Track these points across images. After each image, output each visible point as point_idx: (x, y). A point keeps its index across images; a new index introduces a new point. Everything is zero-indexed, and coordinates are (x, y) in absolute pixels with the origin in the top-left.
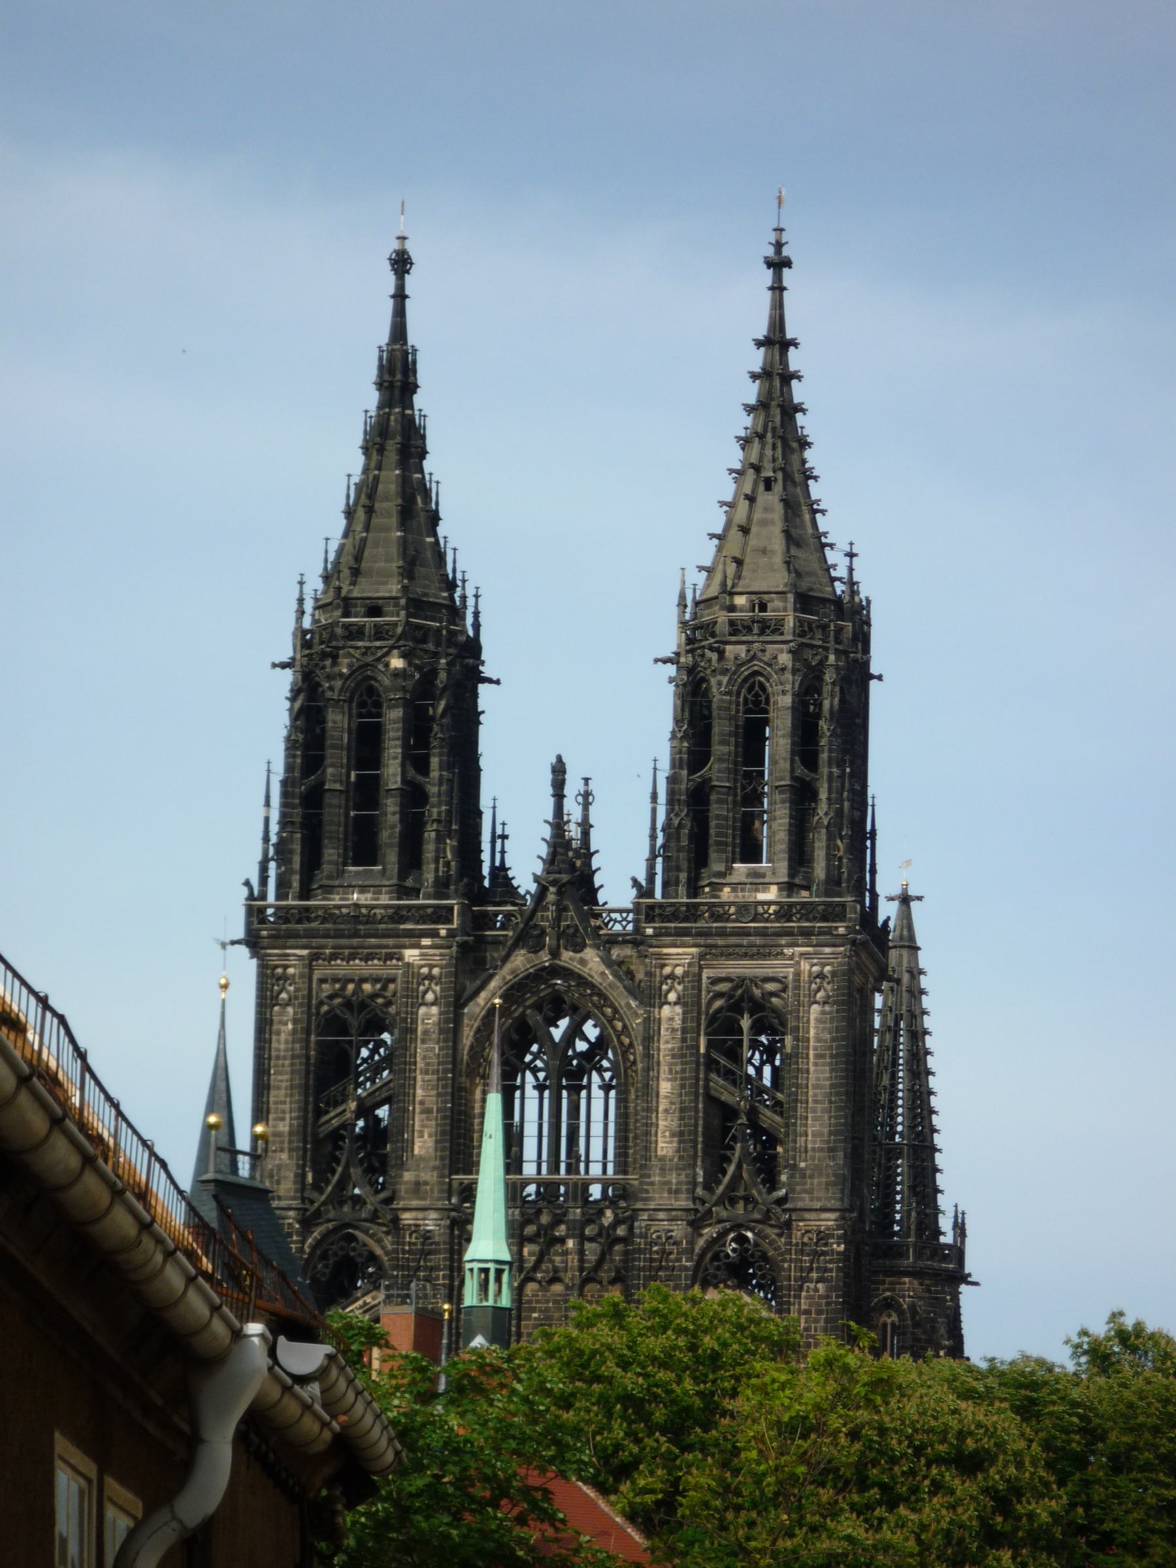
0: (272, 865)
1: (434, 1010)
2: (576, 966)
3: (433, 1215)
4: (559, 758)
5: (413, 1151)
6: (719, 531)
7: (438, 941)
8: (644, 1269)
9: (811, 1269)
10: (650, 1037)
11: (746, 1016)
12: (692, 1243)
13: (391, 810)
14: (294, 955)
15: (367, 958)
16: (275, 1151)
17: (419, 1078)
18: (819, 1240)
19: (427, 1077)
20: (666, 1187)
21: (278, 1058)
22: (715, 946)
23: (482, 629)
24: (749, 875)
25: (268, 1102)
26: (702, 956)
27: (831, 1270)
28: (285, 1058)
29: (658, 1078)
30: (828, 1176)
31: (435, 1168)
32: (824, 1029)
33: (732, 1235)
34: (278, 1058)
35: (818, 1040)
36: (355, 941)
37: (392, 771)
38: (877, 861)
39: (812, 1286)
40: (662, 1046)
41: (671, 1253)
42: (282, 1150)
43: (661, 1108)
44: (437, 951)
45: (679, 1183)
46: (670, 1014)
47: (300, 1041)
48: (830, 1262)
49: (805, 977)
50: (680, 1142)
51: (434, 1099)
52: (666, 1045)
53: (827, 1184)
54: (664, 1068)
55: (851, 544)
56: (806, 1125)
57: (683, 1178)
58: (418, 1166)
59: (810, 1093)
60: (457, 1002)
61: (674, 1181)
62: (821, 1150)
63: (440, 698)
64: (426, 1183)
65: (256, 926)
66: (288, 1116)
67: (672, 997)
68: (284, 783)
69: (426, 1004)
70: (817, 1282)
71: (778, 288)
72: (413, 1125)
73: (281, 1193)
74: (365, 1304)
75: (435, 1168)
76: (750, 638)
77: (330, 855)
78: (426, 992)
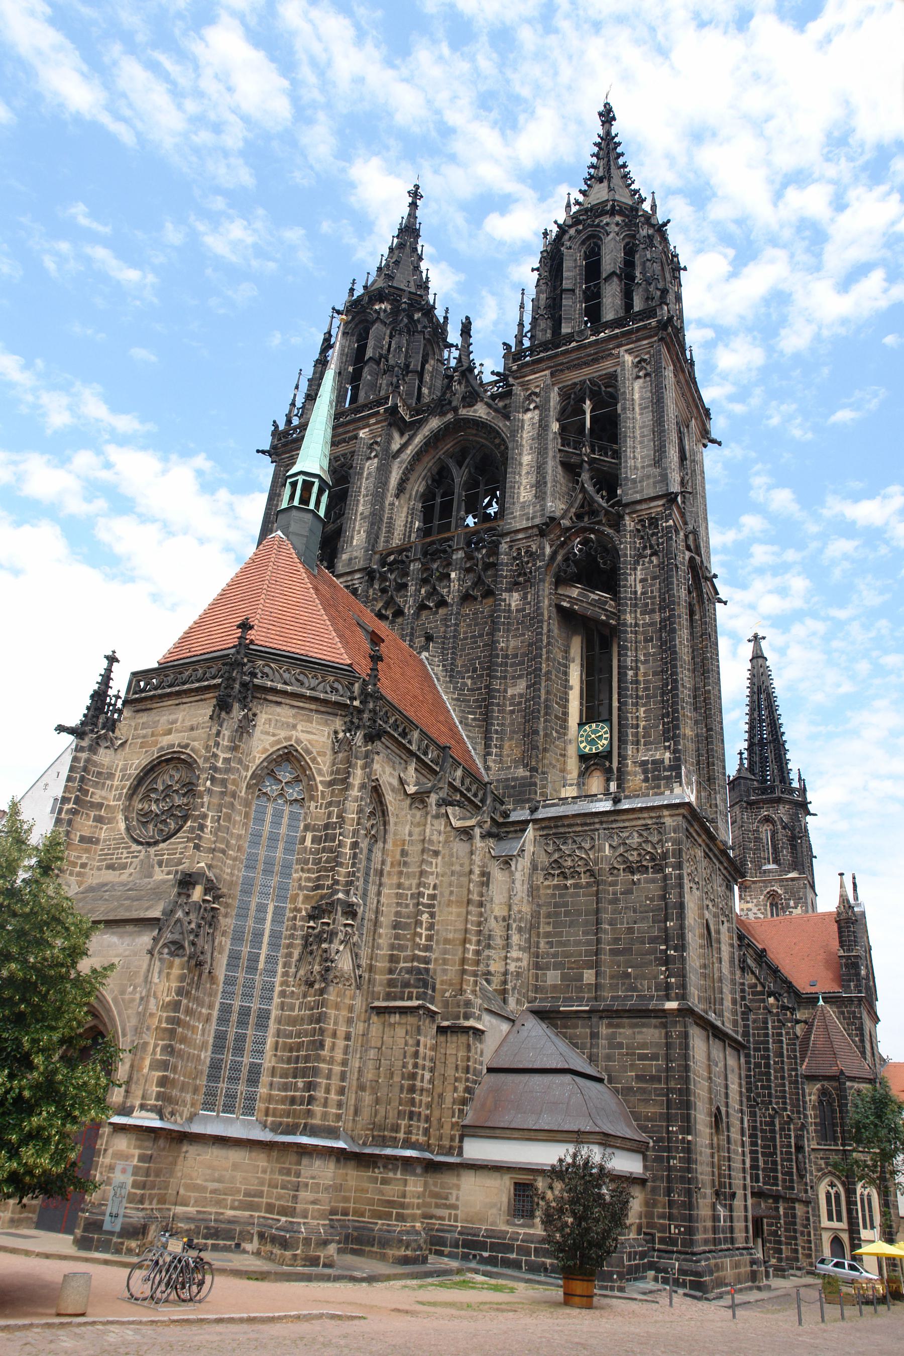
4: (467, 318)
8: (506, 577)
11: (588, 402)
22: (562, 364)
29: (520, 454)
35: (642, 398)
39: (647, 560)
40: (525, 436)
43: (524, 472)
45: (534, 512)
48: (662, 537)
52: (527, 435)
53: (654, 483)
54: (526, 449)
59: (638, 432)
62: (650, 466)
67: (532, 406)
70: (651, 555)
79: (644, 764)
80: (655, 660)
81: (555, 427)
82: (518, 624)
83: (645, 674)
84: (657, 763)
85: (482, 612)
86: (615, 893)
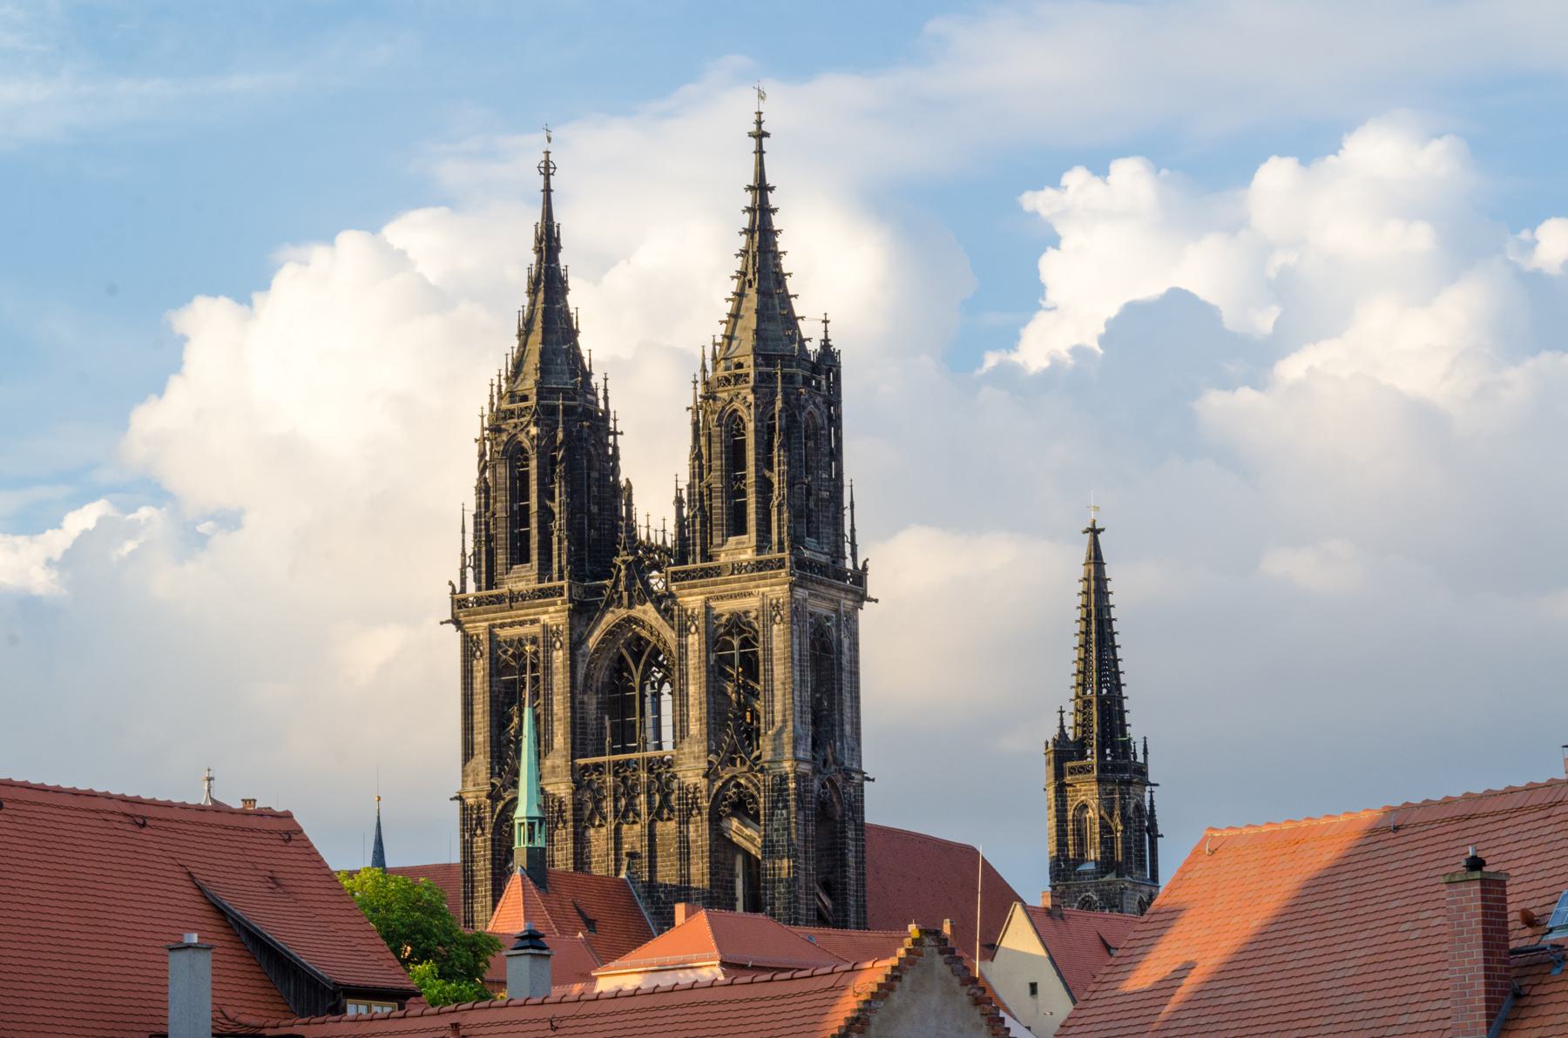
0: (470, 573)
1: (561, 653)
2: (641, 616)
5: (552, 746)
7: (558, 608)
9: (778, 801)
12: (709, 790)
14: (481, 626)
15: (522, 624)
18: (781, 781)
20: (692, 755)
23: (610, 401)
24: (738, 543)
26: (708, 599)
28: (480, 694)
33: (733, 783)
38: (855, 523)
39: (779, 812)
42: (481, 753)
43: (690, 703)
44: (558, 615)
45: (699, 752)
46: (694, 641)
51: (562, 711)
54: (690, 677)
55: (826, 314)
57: (701, 748)
60: (576, 645)
61: (696, 750)
63: (559, 451)
64: (559, 767)
65: (456, 611)
68: (475, 516)
70: (783, 809)
71: (760, 152)
73: (479, 781)
76: (729, 388)
77: (501, 559)
85: (668, 834)
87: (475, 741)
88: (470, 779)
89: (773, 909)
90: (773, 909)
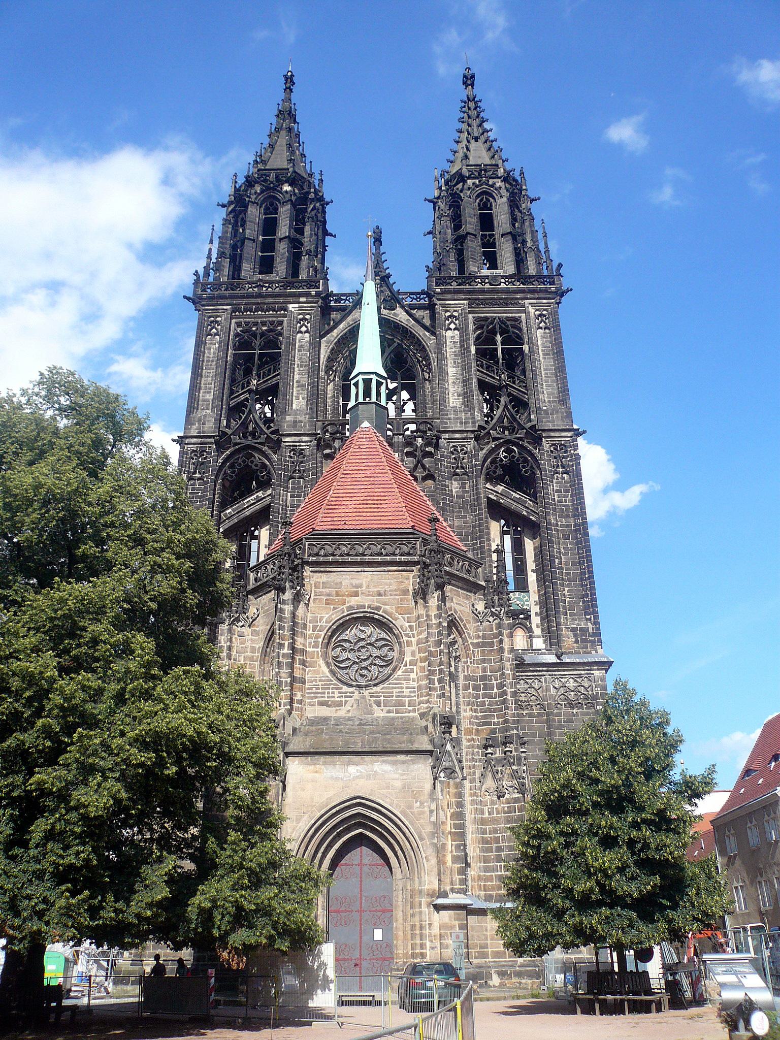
1: (307, 335)
3: (305, 439)
5: (292, 406)
6: (430, 228)
8: (447, 467)
9: (558, 466)
10: (440, 347)
11: (498, 336)
13: (282, 249)
16: (203, 409)
17: (296, 369)
19: (301, 369)
21: (208, 361)
22: (478, 299)
25: (200, 383)
27: (572, 466)
28: (213, 361)
30: (562, 413)
31: (306, 414)
32: (546, 341)
34: (208, 361)
36: (259, 300)
37: (283, 229)
39: (560, 476)
41: (463, 459)
42: (207, 409)
43: (450, 382)
44: (309, 305)
46: (451, 336)
47: (223, 351)
48: (571, 461)
49: (532, 315)
50: (464, 399)
52: (450, 350)
54: (450, 362)
56: (543, 388)
58: (296, 413)
59: (543, 373)
62: (554, 402)
64: (301, 422)
66: (212, 391)
67: (452, 326)
69: (301, 332)
72: (292, 393)
73: (206, 429)
74: (257, 496)
75: (306, 414)
78: (301, 327)
79: (574, 630)
80: (573, 554)
81: (473, 349)
82: (460, 507)
83: (566, 563)
84: (584, 631)
86: (560, 722)
87: (201, 398)
88: (195, 427)
89: (560, 563)
90: (560, 563)
